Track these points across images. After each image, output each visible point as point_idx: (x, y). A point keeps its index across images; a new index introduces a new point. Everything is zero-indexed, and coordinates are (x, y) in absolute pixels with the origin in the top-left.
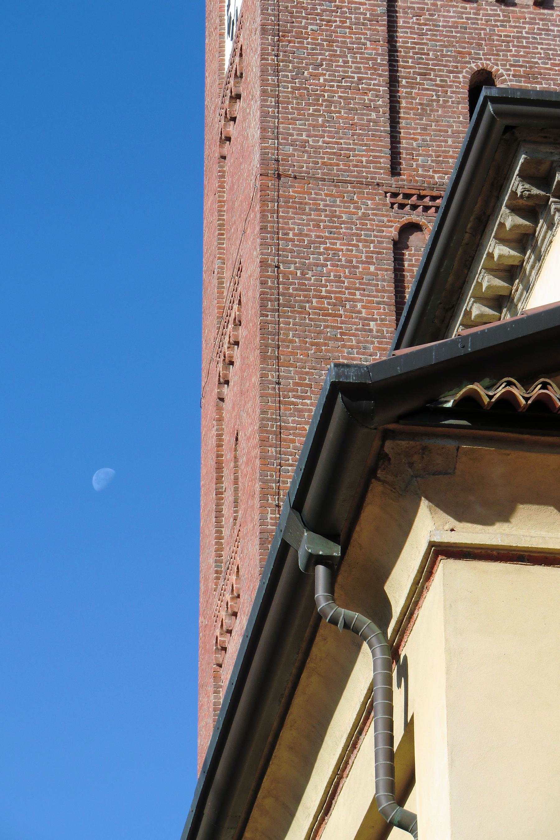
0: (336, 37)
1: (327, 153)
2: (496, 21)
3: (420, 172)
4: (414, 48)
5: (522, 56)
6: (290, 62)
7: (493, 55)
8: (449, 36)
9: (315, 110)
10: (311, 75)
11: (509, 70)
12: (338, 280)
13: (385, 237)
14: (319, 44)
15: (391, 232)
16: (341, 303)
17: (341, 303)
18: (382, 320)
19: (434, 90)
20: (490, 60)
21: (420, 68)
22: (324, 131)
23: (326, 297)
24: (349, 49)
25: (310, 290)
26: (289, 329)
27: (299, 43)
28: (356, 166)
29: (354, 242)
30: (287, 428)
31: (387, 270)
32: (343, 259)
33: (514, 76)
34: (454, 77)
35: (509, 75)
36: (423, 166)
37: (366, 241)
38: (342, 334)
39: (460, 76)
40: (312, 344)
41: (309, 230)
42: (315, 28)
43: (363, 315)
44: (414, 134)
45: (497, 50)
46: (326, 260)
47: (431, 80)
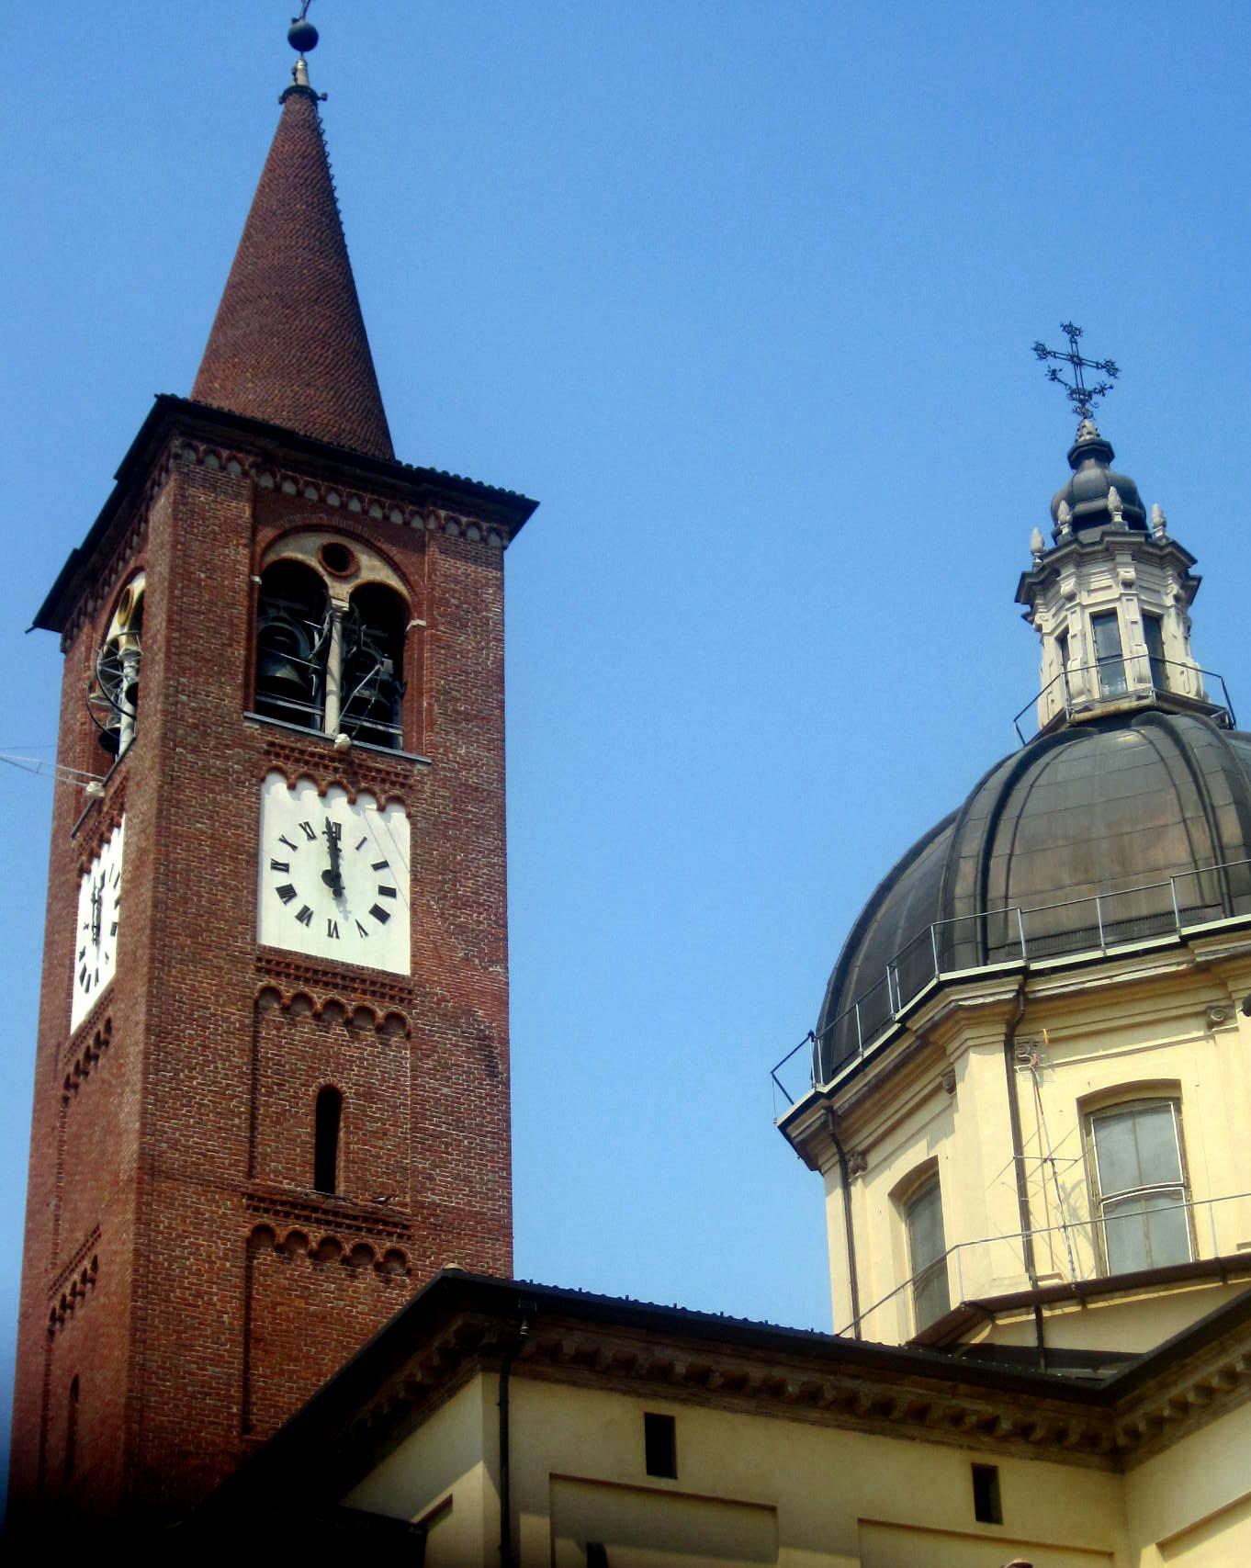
0: (209, 1042)
1: (195, 1153)
2: (343, 1041)
3: (272, 1176)
4: (273, 1059)
5: (363, 1076)
6: (169, 1062)
7: (338, 1072)
8: (302, 1051)
9: (188, 1111)
10: (187, 1076)
11: (350, 1088)
12: (199, 1274)
13: (239, 1236)
14: (194, 1049)
15: (245, 1232)
16: (199, 1295)
17: (199, 1295)
18: (234, 1313)
19: (287, 1101)
20: (335, 1076)
21: (277, 1079)
22: (195, 1132)
23: (188, 1289)
24: (219, 1055)
25: (175, 1281)
26: (156, 1316)
27: (178, 1045)
28: (219, 1167)
29: (214, 1239)
30: (148, 1407)
31: (240, 1268)
32: (204, 1254)
33: (354, 1093)
34: (305, 1090)
35: (350, 1093)
36: (274, 1172)
37: (224, 1239)
38: (200, 1323)
39: (310, 1089)
40: (175, 1331)
41: (177, 1224)
42: (193, 1032)
43: (218, 1307)
44: (268, 1140)
45: (342, 1068)
46: (190, 1254)
47: (285, 1090)
